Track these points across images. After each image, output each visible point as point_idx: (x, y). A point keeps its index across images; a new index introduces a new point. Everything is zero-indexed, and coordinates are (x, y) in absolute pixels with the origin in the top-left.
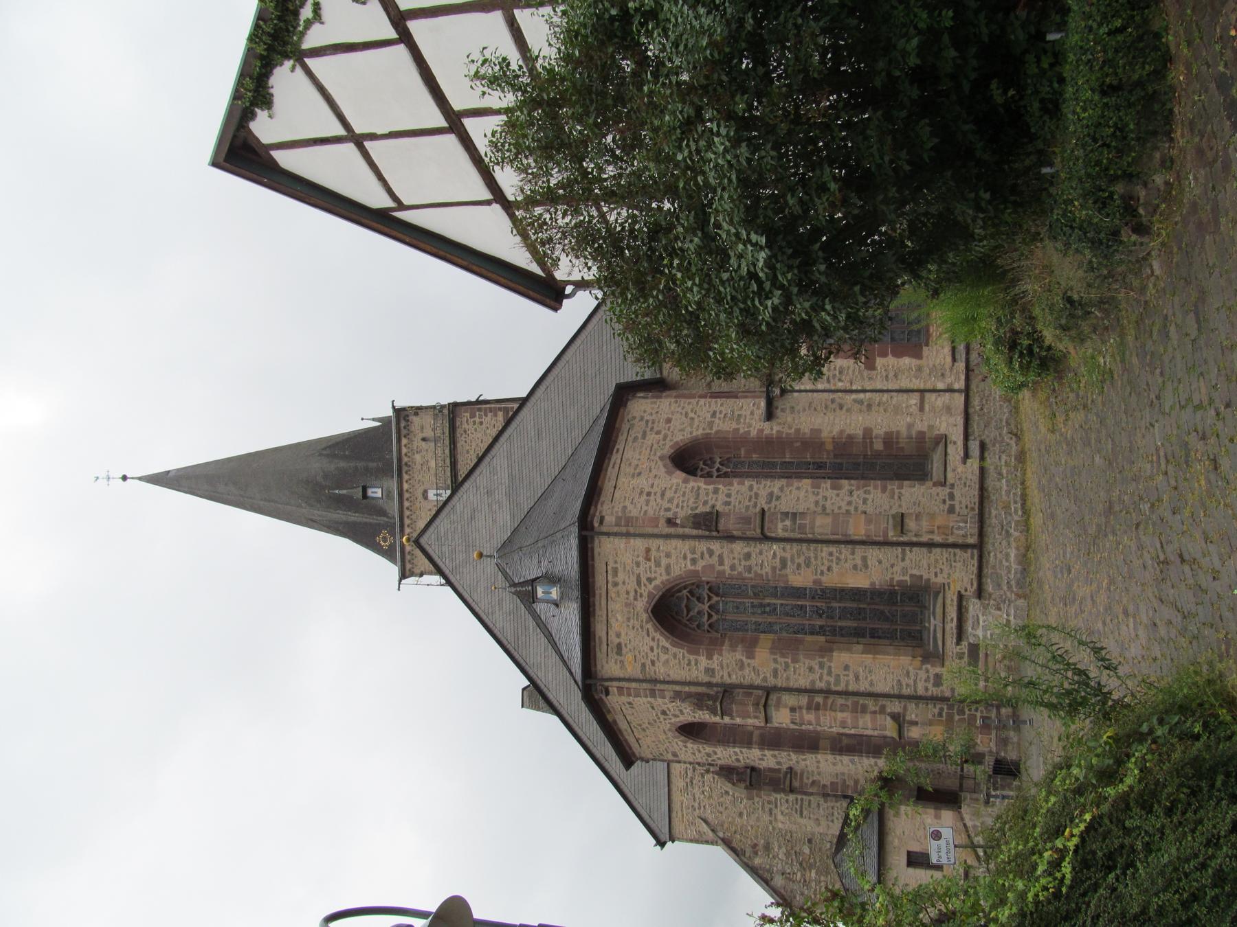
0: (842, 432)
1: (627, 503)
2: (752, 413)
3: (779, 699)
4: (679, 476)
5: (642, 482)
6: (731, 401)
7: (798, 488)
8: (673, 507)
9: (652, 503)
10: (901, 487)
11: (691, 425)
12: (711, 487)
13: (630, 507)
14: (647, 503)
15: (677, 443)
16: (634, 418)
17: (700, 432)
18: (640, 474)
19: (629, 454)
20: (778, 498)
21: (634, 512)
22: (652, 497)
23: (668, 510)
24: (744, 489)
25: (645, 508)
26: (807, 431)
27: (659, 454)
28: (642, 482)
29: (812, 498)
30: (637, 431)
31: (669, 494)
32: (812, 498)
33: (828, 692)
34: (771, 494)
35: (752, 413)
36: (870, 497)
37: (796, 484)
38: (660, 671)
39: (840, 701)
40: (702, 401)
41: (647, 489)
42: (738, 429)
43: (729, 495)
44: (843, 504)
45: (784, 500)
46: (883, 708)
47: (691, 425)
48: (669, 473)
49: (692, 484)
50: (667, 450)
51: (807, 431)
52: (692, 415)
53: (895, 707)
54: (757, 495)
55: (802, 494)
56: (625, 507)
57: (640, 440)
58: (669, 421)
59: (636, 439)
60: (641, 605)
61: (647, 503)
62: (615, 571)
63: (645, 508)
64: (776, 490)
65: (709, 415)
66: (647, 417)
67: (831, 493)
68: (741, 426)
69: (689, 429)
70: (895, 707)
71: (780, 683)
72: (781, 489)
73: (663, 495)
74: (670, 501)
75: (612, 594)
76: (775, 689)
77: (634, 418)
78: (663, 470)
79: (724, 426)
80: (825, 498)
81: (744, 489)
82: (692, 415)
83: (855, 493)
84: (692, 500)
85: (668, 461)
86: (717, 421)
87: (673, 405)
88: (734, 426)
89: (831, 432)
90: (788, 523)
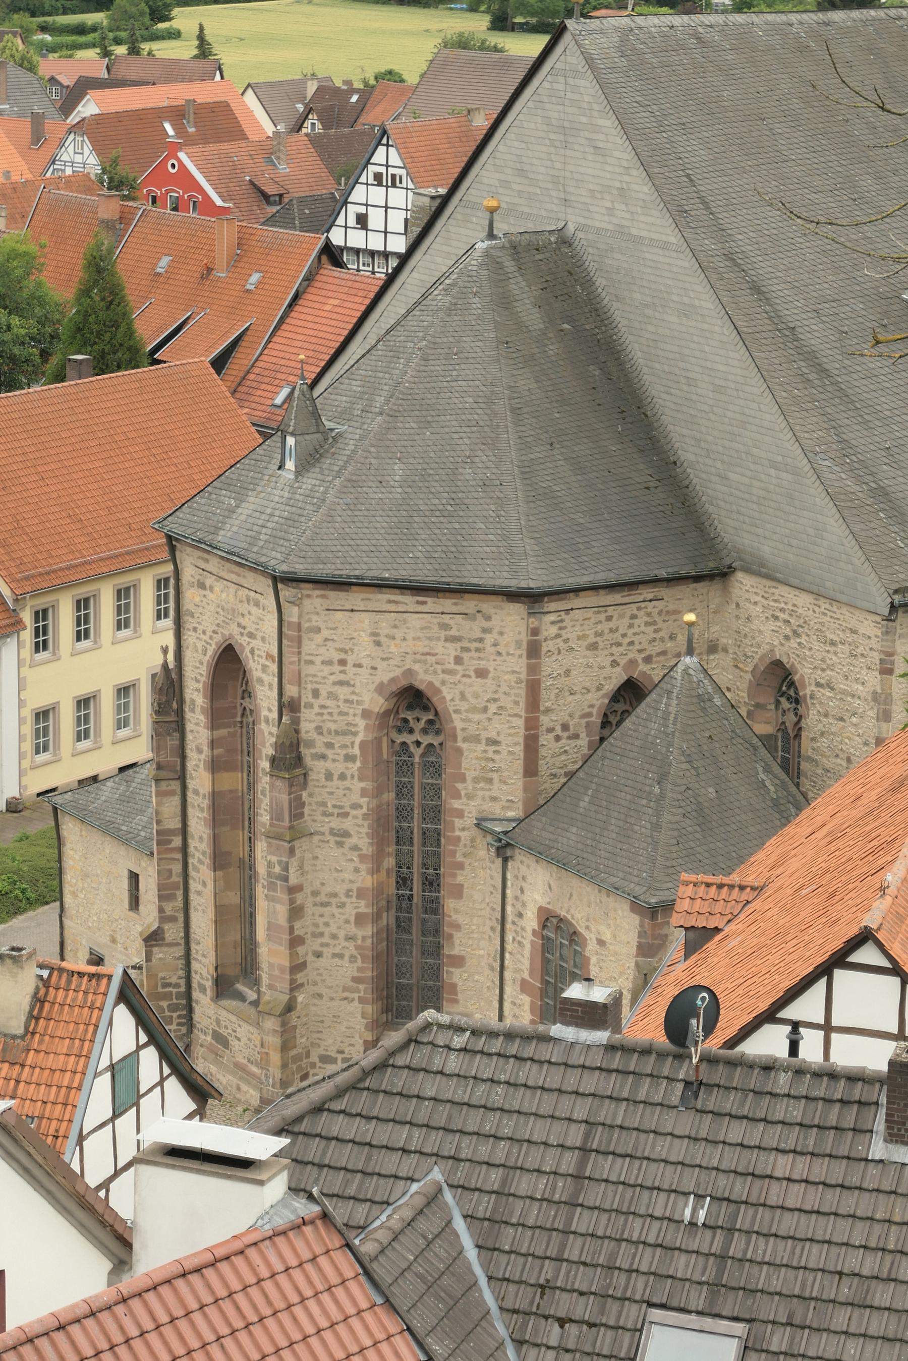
0: (458, 927)
1: (325, 633)
2: (494, 799)
3: (172, 793)
4: (379, 704)
5: (364, 650)
6: (519, 765)
7: (357, 870)
8: (321, 701)
9: (327, 669)
10: (361, 1000)
11: (473, 710)
12: (356, 751)
13: (319, 638)
14: (329, 663)
15: (439, 691)
16: (488, 618)
17: (459, 724)
18: (378, 644)
19: (415, 621)
20: (340, 844)
21: (309, 646)
22: (337, 668)
23: (316, 693)
24: (355, 797)
25: (318, 660)
26: (460, 879)
27: (417, 667)
28: (364, 650)
29: (341, 889)
30: (459, 626)
31: (343, 692)
32: (341, 889)
33: (184, 849)
34: (346, 834)
35: (494, 799)
36: (346, 962)
37: (363, 867)
38: (189, 638)
39: (177, 868)
40: (520, 723)
41: (351, 659)
42: (463, 779)
43: (342, 777)
44: (333, 929)
45: (336, 852)
46: (173, 919)
47: (473, 710)
48: (380, 689)
49: (361, 723)
50: (423, 679)
51: (460, 879)
52: (493, 708)
53: (173, 932)
54: (345, 815)
55: (346, 876)
56: (318, 630)
57: (443, 634)
58: (482, 673)
59: (445, 627)
60: (234, 630)
61: (329, 663)
62: (257, 604)
63: (318, 660)
64: (353, 841)
65: (493, 735)
66: (489, 639)
67: (350, 912)
68: (469, 784)
69: (464, 706)
70: (173, 932)
71: (190, 794)
72: (355, 848)
73: (341, 683)
74: (331, 695)
75: (243, 593)
76: (184, 788)
77: (488, 618)
78: (386, 678)
79: (471, 759)
80: (342, 905)
81: (355, 797)
82: (493, 708)
83: (351, 945)
84: (333, 727)
85: (404, 683)
86: (482, 747)
87: (513, 678)
88: (470, 775)
89: (457, 911)
90: (277, 869)
